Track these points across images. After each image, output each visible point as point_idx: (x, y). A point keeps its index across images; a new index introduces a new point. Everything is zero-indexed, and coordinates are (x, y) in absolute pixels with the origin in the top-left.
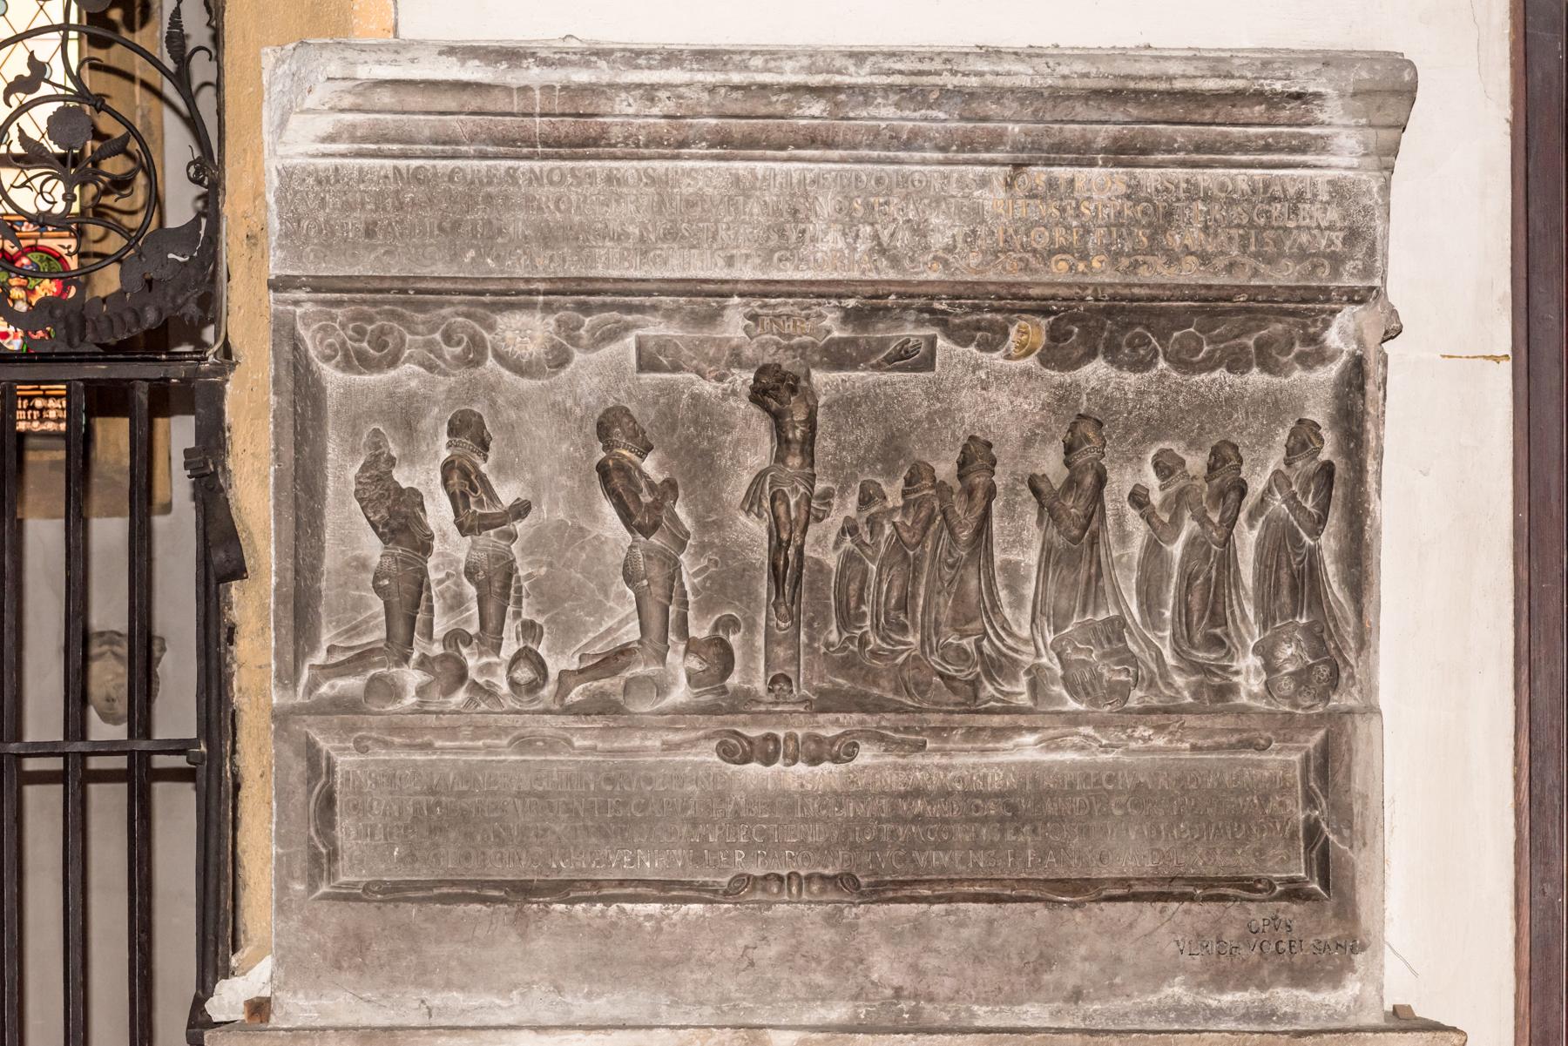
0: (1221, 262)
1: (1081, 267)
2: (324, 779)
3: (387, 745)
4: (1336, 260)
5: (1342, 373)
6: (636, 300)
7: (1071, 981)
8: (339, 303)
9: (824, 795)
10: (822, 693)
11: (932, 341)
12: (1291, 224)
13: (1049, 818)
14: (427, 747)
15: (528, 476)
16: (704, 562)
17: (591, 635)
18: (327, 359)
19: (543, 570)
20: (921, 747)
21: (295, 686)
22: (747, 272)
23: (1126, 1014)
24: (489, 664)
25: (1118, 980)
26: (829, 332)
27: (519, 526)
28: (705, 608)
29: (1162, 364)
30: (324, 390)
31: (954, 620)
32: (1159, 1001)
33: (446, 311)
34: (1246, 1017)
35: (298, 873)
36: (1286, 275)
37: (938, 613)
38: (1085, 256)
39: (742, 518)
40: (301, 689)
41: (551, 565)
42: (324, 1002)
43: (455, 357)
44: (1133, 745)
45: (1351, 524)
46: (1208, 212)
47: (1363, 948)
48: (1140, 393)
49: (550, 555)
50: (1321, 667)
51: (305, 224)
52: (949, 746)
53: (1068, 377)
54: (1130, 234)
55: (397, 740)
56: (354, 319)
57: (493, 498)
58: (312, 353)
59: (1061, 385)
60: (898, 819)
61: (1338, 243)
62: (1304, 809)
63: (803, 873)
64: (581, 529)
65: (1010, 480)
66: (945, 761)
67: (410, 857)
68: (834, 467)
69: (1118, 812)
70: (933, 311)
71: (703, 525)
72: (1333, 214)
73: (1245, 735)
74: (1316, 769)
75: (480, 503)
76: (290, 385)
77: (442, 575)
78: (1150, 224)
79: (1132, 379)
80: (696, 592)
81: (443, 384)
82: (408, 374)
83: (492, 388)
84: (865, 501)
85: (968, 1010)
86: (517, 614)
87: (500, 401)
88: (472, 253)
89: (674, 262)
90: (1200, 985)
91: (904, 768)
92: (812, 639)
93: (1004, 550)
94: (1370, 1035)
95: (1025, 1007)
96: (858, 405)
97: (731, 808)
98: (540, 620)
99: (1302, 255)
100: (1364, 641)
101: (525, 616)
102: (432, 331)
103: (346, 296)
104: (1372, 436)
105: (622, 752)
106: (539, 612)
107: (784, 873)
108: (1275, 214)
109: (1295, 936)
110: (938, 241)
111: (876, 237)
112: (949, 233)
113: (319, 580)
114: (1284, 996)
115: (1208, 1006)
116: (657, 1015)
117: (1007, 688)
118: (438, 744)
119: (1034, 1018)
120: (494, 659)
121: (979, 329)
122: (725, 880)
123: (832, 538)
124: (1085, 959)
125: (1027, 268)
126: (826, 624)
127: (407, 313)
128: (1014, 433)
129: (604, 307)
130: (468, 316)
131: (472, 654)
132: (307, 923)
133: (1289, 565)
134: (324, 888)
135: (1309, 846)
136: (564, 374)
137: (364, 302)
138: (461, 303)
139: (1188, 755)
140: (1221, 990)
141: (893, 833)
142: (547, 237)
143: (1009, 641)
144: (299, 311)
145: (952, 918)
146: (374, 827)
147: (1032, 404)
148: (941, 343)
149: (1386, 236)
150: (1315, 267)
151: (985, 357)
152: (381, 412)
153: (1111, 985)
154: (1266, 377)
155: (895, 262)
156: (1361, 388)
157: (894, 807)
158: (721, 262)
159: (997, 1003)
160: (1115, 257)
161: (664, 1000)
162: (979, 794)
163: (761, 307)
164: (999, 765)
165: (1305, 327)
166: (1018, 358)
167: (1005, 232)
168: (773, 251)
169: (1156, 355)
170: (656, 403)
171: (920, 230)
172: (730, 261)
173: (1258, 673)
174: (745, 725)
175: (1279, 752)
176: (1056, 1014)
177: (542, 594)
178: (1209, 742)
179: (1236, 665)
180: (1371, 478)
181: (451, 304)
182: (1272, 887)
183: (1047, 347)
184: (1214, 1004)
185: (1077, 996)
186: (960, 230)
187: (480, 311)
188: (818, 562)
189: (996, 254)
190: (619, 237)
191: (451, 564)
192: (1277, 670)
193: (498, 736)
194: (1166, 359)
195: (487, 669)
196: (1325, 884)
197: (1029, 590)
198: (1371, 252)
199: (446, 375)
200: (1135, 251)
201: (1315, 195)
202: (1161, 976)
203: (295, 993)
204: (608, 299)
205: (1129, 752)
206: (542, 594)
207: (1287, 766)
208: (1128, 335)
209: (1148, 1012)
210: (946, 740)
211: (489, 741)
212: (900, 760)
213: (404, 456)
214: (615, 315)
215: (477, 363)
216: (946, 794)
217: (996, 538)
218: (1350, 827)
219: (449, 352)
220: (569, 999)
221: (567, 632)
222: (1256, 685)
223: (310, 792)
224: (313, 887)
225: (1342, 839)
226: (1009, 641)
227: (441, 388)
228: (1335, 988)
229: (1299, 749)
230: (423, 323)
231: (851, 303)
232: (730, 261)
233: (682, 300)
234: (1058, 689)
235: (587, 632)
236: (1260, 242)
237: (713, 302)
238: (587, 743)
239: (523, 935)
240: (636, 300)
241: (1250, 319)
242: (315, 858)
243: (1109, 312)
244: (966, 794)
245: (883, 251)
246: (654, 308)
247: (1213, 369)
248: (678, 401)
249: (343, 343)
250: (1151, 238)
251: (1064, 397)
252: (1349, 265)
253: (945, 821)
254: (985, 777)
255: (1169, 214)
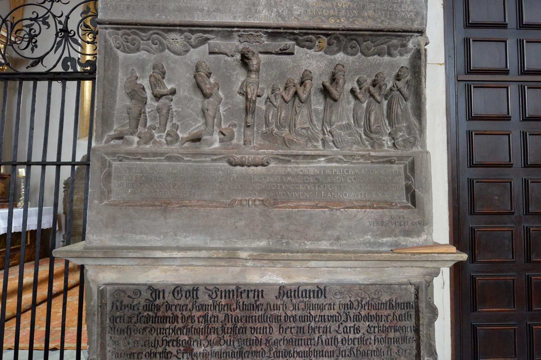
0: (379, 21)
1: (338, 21)
2: (107, 169)
3: (128, 159)
4: (413, 21)
5: (412, 56)
6: (206, 29)
7: (337, 234)
8: (118, 29)
9: (260, 175)
10: (260, 145)
11: (294, 46)
12: (399, 10)
13: (329, 183)
14: (139, 159)
15: (177, 83)
16: (227, 107)
17: (193, 128)
18: (118, 48)
19: (180, 109)
20: (289, 161)
21: (102, 141)
22: (239, 21)
23: (353, 244)
24: (161, 135)
25: (350, 234)
26: (264, 42)
27: (174, 98)
28: (227, 120)
29: (359, 54)
30: (118, 57)
31: (300, 123)
32: (364, 240)
33: (151, 32)
34: (391, 245)
35: (96, 197)
36: (398, 25)
37: (295, 121)
38: (339, 19)
39: (238, 95)
40: (103, 142)
41: (182, 108)
42: (102, 238)
43: (156, 48)
44: (354, 161)
45: (416, 98)
46: (375, 7)
47: (427, 224)
48: (353, 62)
49: (182, 105)
50: (411, 138)
51: (109, 5)
52: (298, 161)
53: (332, 57)
54: (352, 12)
55: (130, 157)
56: (124, 34)
57: (165, 87)
58: (113, 45)
59: (331, 59)
60: (283, 182)
61: (413, 16)
62: (405, 181)
63: (253, 199)
64: (192, 98)
65: (316, 85)
66: (297, 165)
67: (134, 193)
68: (265, 81)
69: (349, 181)
70: (294, 34)
71: (226, 97)
72: (411, 7)
73: (388, 159)
74: (410, 169)
75: (160, 88)
76: (103, 52)
77: (150, 110)
78: (358, 9)
79: (351, 58)
80: (224, 117)
81: (153, 57)
82: (143, 54)
83: (167, 58)
84: (273, 92)
85: (304, 243)
86: (172, 121)
87: (170, 62)
88: (158, 14)
89: (217, 18)
90: (376, 235)
91: (285, 167)
92: (258, 130)
93: (314, 105)
94: (436, 255)
95: (322, 242)
96: (272, 64)
97: (231, 179)
98: (178, 123)
99: (403, 19)
100: (422, 131)
101: (174, 122)
102: (149, 39)
103: (120, 26)
104: (424, 71)
105: (199, 162)
106: (178, 121)
107: (247, 199)
108: (395, 7)
109: (405, 220)
110: (296, 13)
111: (278, 11)
112: (299, 11)
113: (114, 111)
114: (403, 240)
115: (379, 242)
116: (206, 243)
117: (315, 144)
118: (143, 158)
119: (325, 245)
120: (163, 134)
121: (307, 41)
122: (229, 201)
123: (264, 101)
124: (341, 227)
125: (322, 21)
126: (262, 126)
127: (140, 33)
128: (317, 72)
129: (198, 31)
130: (157, 34)
131: (156, 132)
132: (98, 213)
133: (401, 108)
134: (105, 202)
135: (407, 192)
136: (188, 54)
137: (125, 28)
138: (154, 29)
139: (369, 165)
140: (383, 237)
141: (281, 186)
142: (180, 10)
143: (316, 131)
144: (107, 31)
145: (300, 213)
146: (123, 183)
147: (322, 64)
148: (296, 46)
149: (426, 15)
150: (406, 22)
151: (309, 51)
152: (135, 64)
153: (349, 235)
154: (389, 58)
155: (283, 19)
156: (420, 58)
157: (282, 178)
158: (232, 18)
159: (313, 241)
160: (348, 19)
161: (209, 239)
162: (308, 175)
163: (244, 31)
164: (313, 167)
165: (402, 40)
166: (318, 51)
167: (316, 10)
168: (247, 15)
169: (358, 51)
170: (214, 62)
171: (290, 10)
172: (235, 18)
173: (390, 141)
174: (236, 154)
175: (397, 164)
176: (331, 244)
177: (180, 116)
178: (377, 161)
179: (384, 138)
180: (423, 83)
181: (152, 29)
182: (396, 205)
183: (327, 48)
184: (380, 241)
185: (338, 239)
186: (302, 10)
187: (160, 32)
188: (260, 108)
189: (313, 17)
190: (202, 10)
191: (153, 107)
192: (398, 139)
193: (161, 156)
194: (361, 52)
195: (160, 137)
196: (414, 203)
197: (321, 116)
198: (423, 18)
199: (154, 54)
200: (354, 17)
201: (406, 2)
202: (365, 232)
203: (93, 235)
204: (198, 28)
205: (352, 163)
206: (180, 116)
207: (400, 168)
208: (351, 44)
209: (360, 244)
210: (297, 159)
211: (158, 158)
212: (283, 165)
213: (141, 76)
214: (201, 34)
215: (163, 50)
216: (297, 175)
217: (313, 102)
218: (422, 187)
219: (154, 46)
220: (179, 238)
221: (186, 127)
222: (390, 143)
223: (102, 172)
224: (101, 201)
225: (419, 191)
226: (316, 131)
227: (153, 57)
228: (418, 237)
229: (404, 163)
230: (145, 36)
231: (270, 31)
232: (235, 18)
233: (220, 29)
234: (331, 144)
235: (192, 127)
236: (390, 15)
237: (229, 29)
238: (188, 159)
239: (165, 218)
240: (206, 29)
241: (387, 38)
242: (103, 193)
243: (345, 36)
244: (304, 175)
245: (280, 16)
246: (212, 31)
247: (374, 55)
248: (221, 62)
249: (122, 43)
250: (358, 13)
251: (331, 62)
252: (416, 22)
253: (297, 183)
254: (308, 171)
255: (363, 7)
